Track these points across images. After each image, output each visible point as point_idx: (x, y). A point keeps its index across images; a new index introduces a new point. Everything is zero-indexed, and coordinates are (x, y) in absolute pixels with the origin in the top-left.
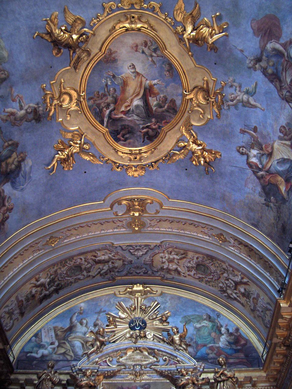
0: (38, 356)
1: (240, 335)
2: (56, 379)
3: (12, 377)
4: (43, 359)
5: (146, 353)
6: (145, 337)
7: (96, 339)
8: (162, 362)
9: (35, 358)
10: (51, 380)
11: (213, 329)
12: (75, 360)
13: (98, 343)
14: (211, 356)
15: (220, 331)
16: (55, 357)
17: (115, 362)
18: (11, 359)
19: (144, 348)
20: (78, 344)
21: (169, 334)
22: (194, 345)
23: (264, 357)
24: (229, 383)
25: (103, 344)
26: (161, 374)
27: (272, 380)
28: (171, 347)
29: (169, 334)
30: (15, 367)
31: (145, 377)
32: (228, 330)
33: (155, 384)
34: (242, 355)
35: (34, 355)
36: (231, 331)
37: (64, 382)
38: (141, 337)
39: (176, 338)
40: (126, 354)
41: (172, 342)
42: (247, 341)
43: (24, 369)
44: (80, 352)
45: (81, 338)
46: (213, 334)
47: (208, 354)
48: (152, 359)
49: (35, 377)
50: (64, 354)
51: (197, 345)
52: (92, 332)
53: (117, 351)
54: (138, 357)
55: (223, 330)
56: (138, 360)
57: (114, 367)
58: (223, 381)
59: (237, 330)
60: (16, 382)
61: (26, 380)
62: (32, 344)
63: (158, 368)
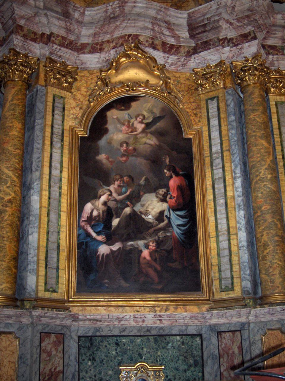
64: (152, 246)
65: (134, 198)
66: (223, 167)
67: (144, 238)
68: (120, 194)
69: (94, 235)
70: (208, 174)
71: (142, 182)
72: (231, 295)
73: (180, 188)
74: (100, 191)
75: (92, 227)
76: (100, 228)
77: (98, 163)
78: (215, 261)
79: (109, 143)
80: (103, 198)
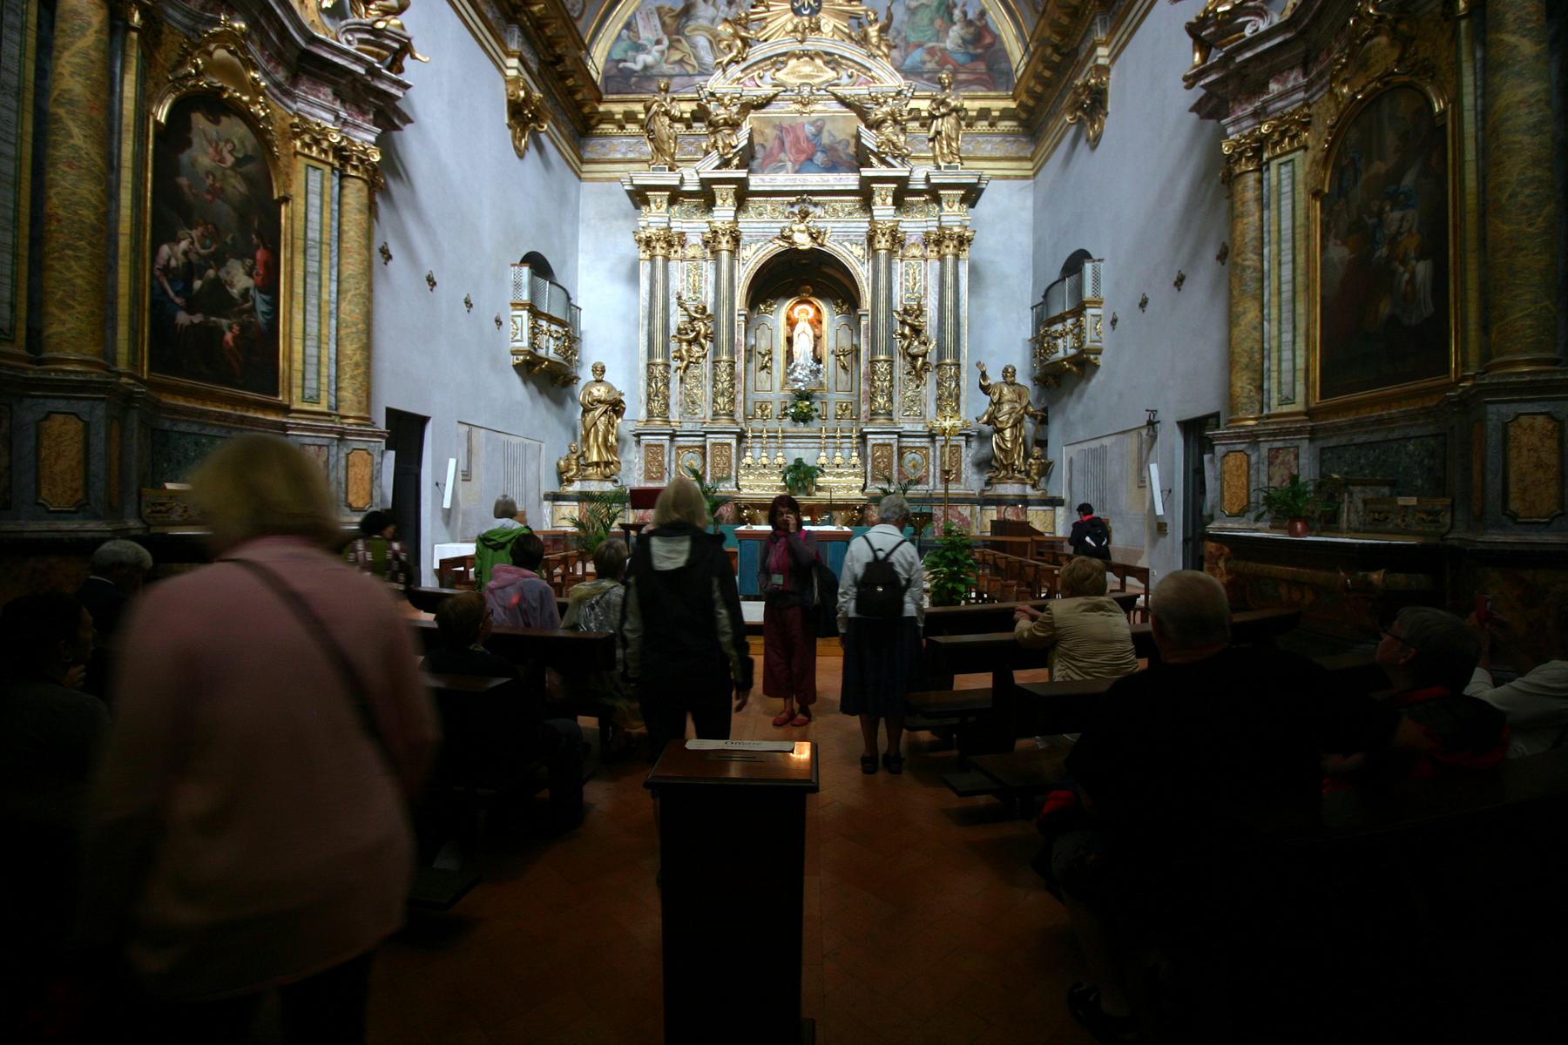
0: (638, 67)
1: (986, 26)
2: (675, 112)
3: (602, 108)
4: (647, 73)
5: (819, 62)
6: (819, 29)
7: (736, 35)
8: (845, 80)
9: (633, 72)
10: (666, 113)
11: (938, 9)
12: (701, 74)
13: (739, 43)
14: (930, 66)
15: (951, 15)
16: (666, 68)
17: (768, 78)
18: (594, 75)
19: (817, 54)
20: (702, 41)
21: (860, 25)
22: (902, 44)
23: (1020, 73)
24: (951, 120)
25: (746, 43)
26: (842, 101)
27: (1023, 116)
28: (863, 51)
29: (860, 25)
30: (602, 89)
31: (818, 107)
32: (965, 14)
33: (833, 119)
34: (982, 67)
35: (630, 65)
36: (970, 16)
37: (687, 115)
38: (812, 30)
39: (873, 31)
40: (785, 63)
41: (863, 41)
42: (997, 38)
43: (618, 93)
44: (709, 59)
45: (707, 30)
46: (938, 23)
47: (924, 63)
48: (830, 74)
49: (639, 107)
50: (681, 62)
51: (908, 44)
52: (726, 20)
53: (770, 58)
54: (807, 69)
55: (957, 13)
56: (806, 76)
57: (767, 90)
58: (943, 116)
59: (983, 14)
60: (608, 118)
61: (625, 113)
62: (623, 45)
63: (839, 91)
64: (236, 328)
65: (219, 260)
66: (320, 262)
67: (226, 317)
68: (203, 247)
69: (171, 294)
70: (299, 260)
71: (228, 240)
72: (316, 408)
73: (266, 265)
74: (181, 233)
75: (170, 281)
76: (180, 286)
77: (178, 187)
78: (298, 365)
79: (193, 163)
80: (184, 245)
